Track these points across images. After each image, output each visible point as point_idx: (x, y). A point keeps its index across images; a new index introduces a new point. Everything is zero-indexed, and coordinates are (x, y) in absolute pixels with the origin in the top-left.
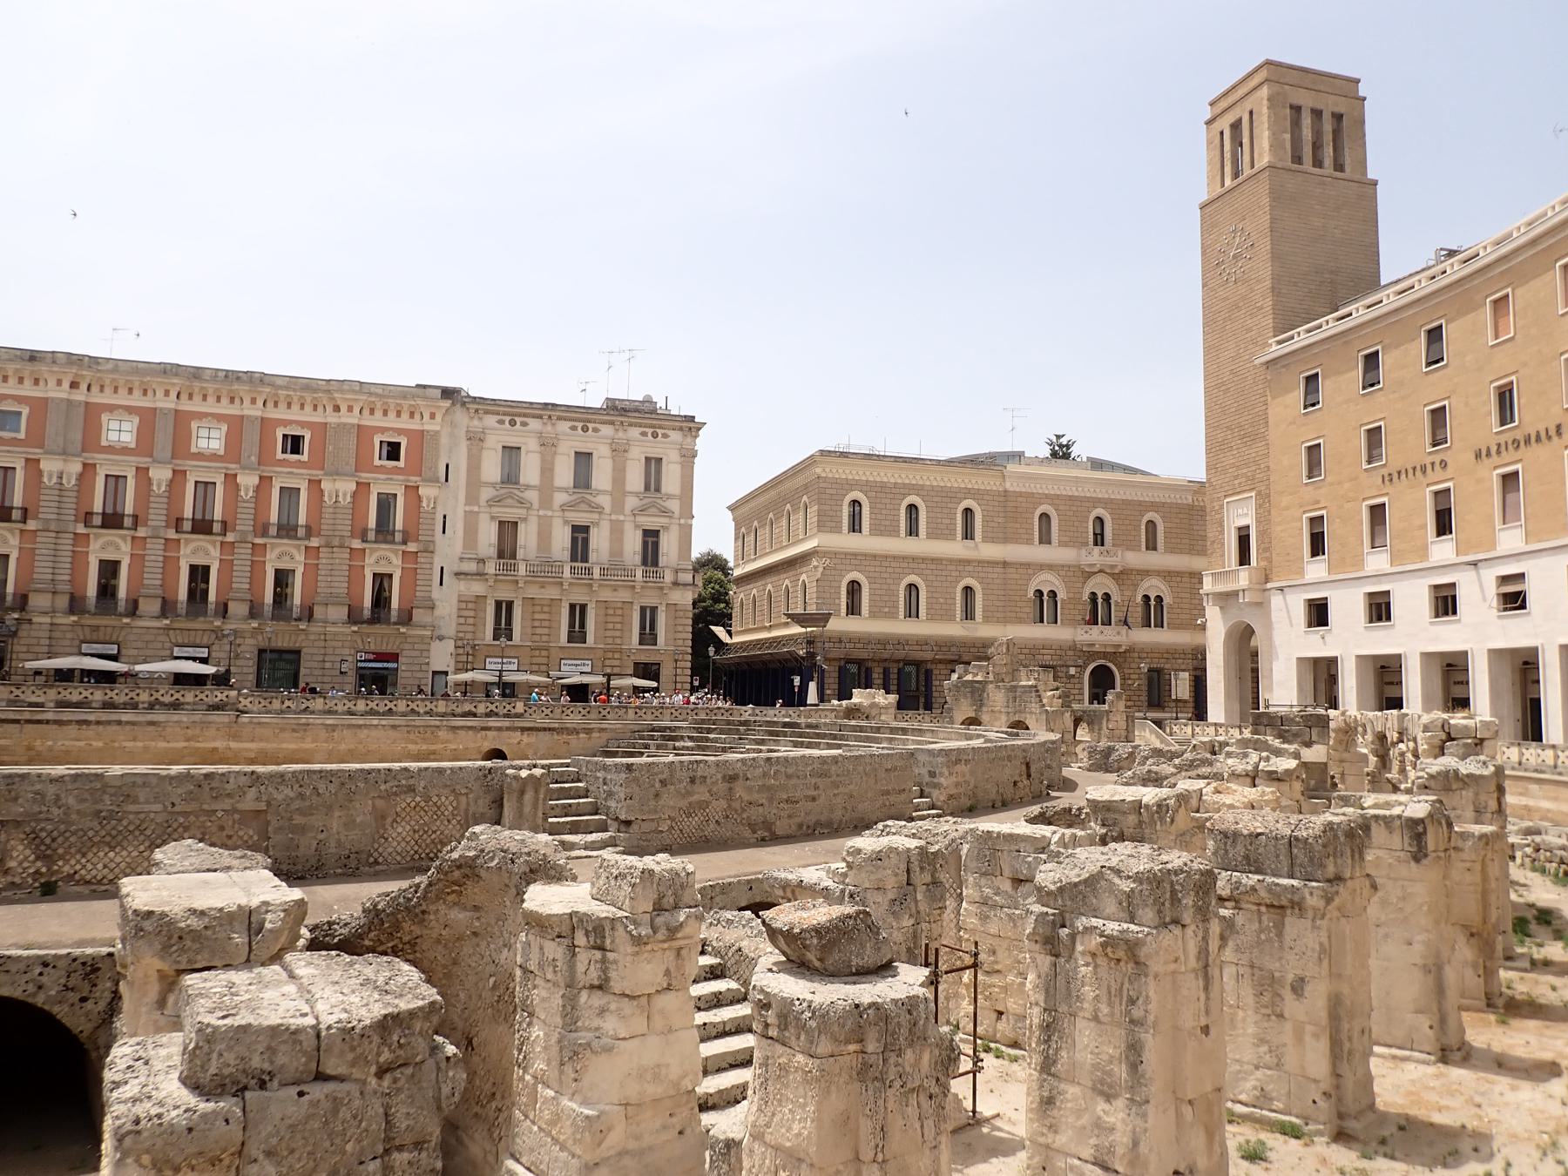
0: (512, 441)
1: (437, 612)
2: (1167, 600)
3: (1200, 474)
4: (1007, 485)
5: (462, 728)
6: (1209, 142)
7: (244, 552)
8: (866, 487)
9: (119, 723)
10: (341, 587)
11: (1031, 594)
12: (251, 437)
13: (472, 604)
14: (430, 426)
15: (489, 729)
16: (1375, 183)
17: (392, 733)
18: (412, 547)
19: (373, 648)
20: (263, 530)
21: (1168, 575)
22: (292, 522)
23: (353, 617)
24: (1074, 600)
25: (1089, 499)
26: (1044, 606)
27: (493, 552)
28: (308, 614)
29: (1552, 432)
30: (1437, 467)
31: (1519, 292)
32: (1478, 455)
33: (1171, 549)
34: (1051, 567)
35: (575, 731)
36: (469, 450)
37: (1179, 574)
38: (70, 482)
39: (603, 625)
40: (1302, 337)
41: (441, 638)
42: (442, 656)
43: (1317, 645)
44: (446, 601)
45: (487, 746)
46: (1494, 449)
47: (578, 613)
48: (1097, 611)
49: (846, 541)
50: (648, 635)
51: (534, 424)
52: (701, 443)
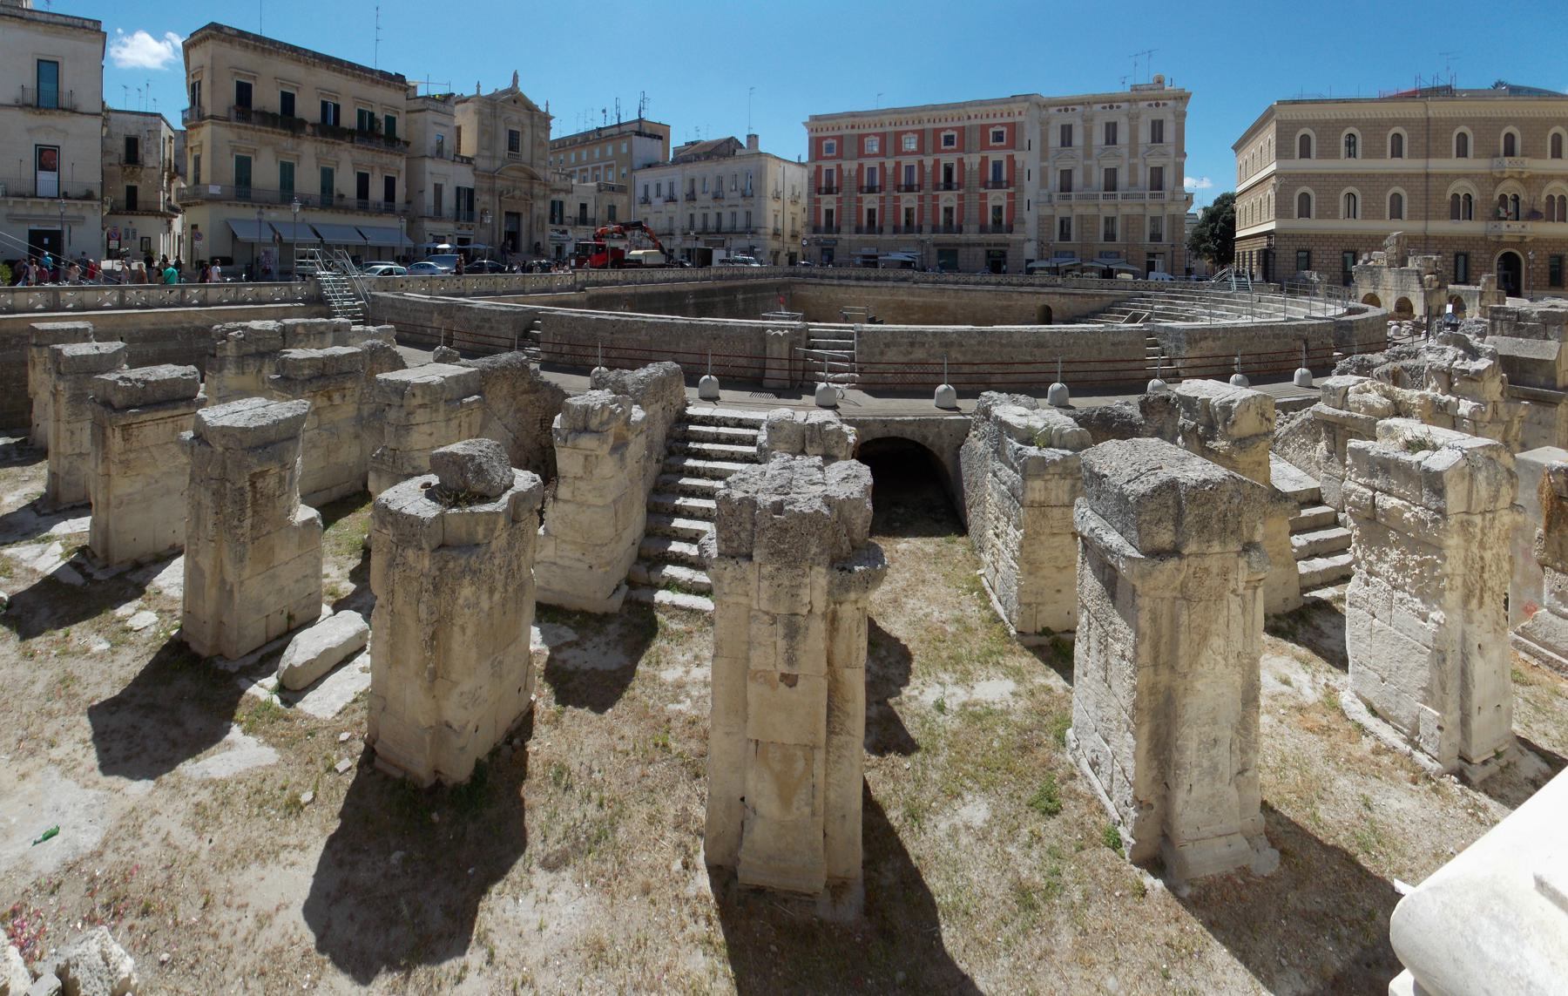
4: (1431, 113)
7: (928, 200)
8: (1312, 124)
10: (975, 213)
11: (1449, 197)
12: (929, 140)
13: (1043, 221)
14: (1018, 119)
18: (1011, 190)
20: (936, 187)
23: (983, 229)
26: (1462, 207)
28: (960, 230)
34: (1466, 176)
38: (854, 173)
42: (1030, 250)
44: (1030, 217)
49: (1299, 165)
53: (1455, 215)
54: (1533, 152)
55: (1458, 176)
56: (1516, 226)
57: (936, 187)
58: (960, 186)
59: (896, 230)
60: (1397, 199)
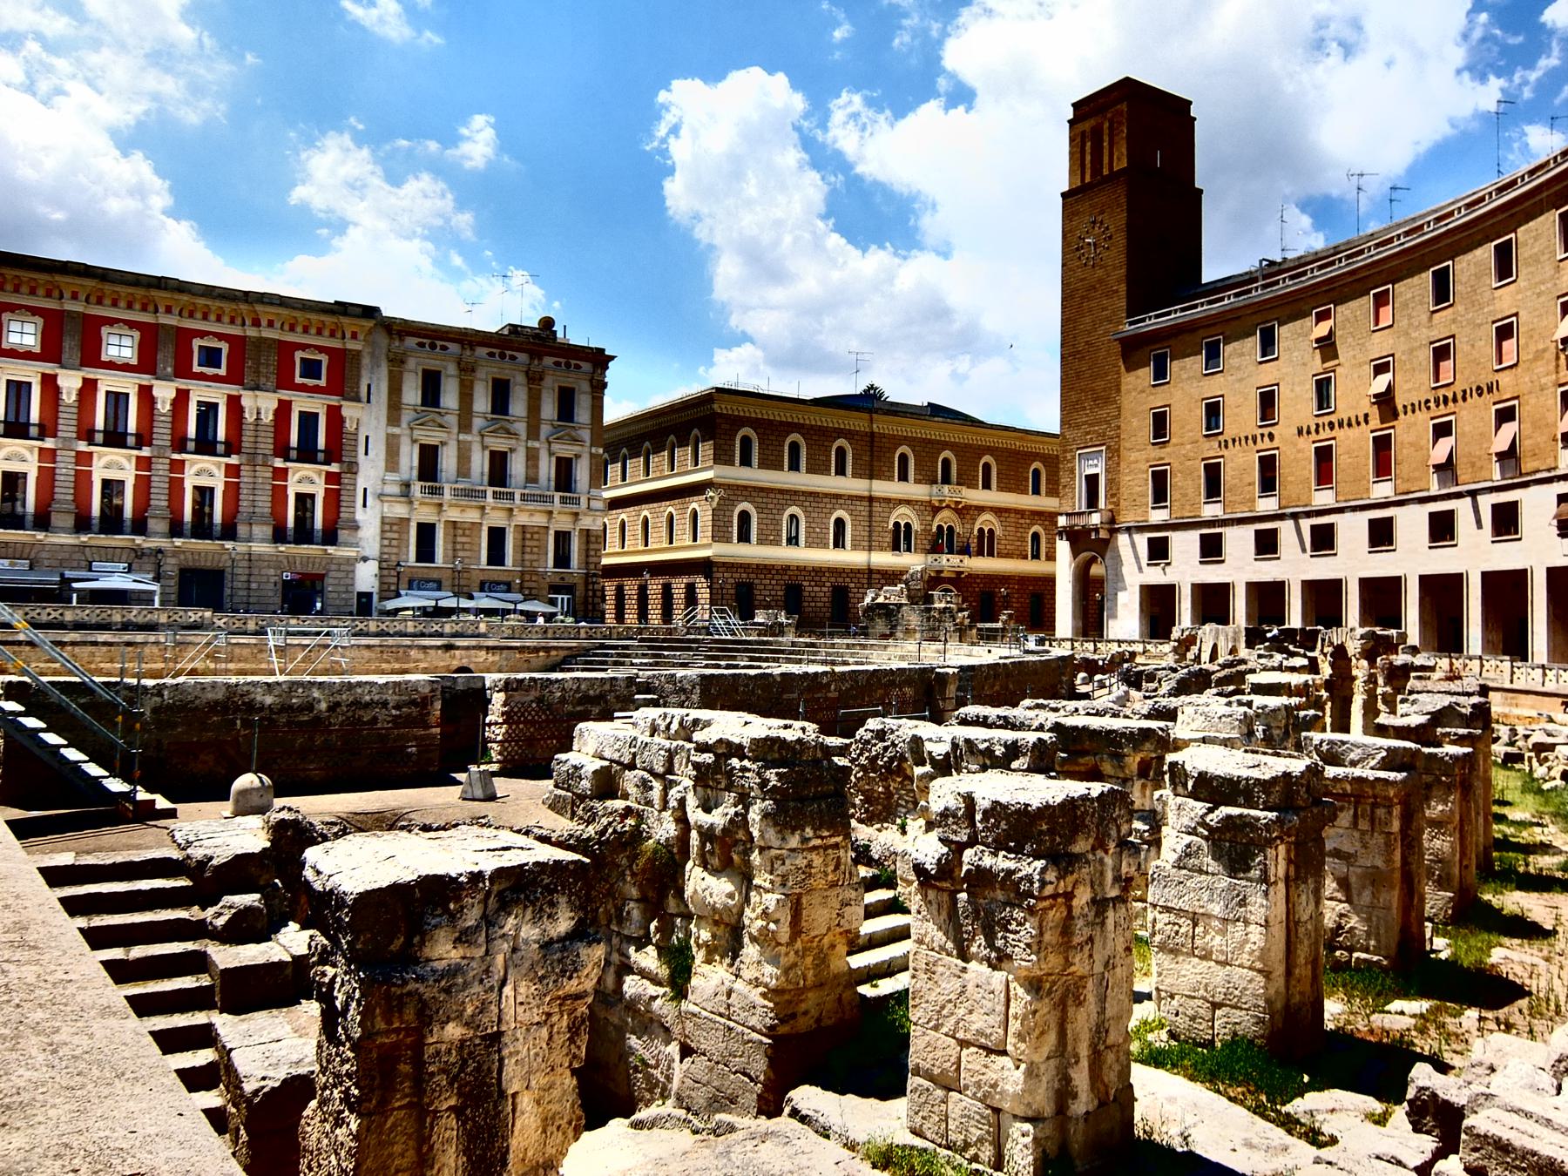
0: (433, 364)
1: (361, 534)
2: (998, 532)
3: (1056, 429)
5: (431, 647)
6: (1072, 140)
7: (161, 468)
8: (755, 423)
9: (95, 644)
10: (264, 503)
11: (891, 526)
13: (392, 527)
14: (352, 345)
15: (458, 648)
16: (1201, 191)
17: (366, 654)
18: (334, 468)
19: (299, 569)
21: (999, 511)
22: (22, 420)
23: (279, 536)
24: (927, 531)
25: (939, 442)
27: (415, 473)
29: (1361, 419)
30: (1266, 439)
31: (1339, 308)
32: (1300, 432)
33: (1000, 489)
34: (908, 502)
35: (536, 650)
36: (390, 372)
37: (1007, 510)
39: (522, 548)
40: (1153, 322)
41: (365, 559)
42: (366, 578)
43: (1155, 576)
44: (368, 520)
45: (456, 664)
46: (1313, 428)
47: (497, 536)
48: (941, 542)
50: (562, 559)
51: (454, 348)
52: (612, 374)
53: (896, 547)
54: (967, 481)
55: (901, 502)
56: (955, 560)
57: (179, 444)
58: (232, 447)
59: (82, 523)
60: (840, 523)
